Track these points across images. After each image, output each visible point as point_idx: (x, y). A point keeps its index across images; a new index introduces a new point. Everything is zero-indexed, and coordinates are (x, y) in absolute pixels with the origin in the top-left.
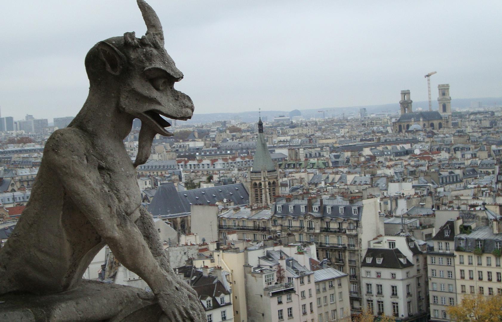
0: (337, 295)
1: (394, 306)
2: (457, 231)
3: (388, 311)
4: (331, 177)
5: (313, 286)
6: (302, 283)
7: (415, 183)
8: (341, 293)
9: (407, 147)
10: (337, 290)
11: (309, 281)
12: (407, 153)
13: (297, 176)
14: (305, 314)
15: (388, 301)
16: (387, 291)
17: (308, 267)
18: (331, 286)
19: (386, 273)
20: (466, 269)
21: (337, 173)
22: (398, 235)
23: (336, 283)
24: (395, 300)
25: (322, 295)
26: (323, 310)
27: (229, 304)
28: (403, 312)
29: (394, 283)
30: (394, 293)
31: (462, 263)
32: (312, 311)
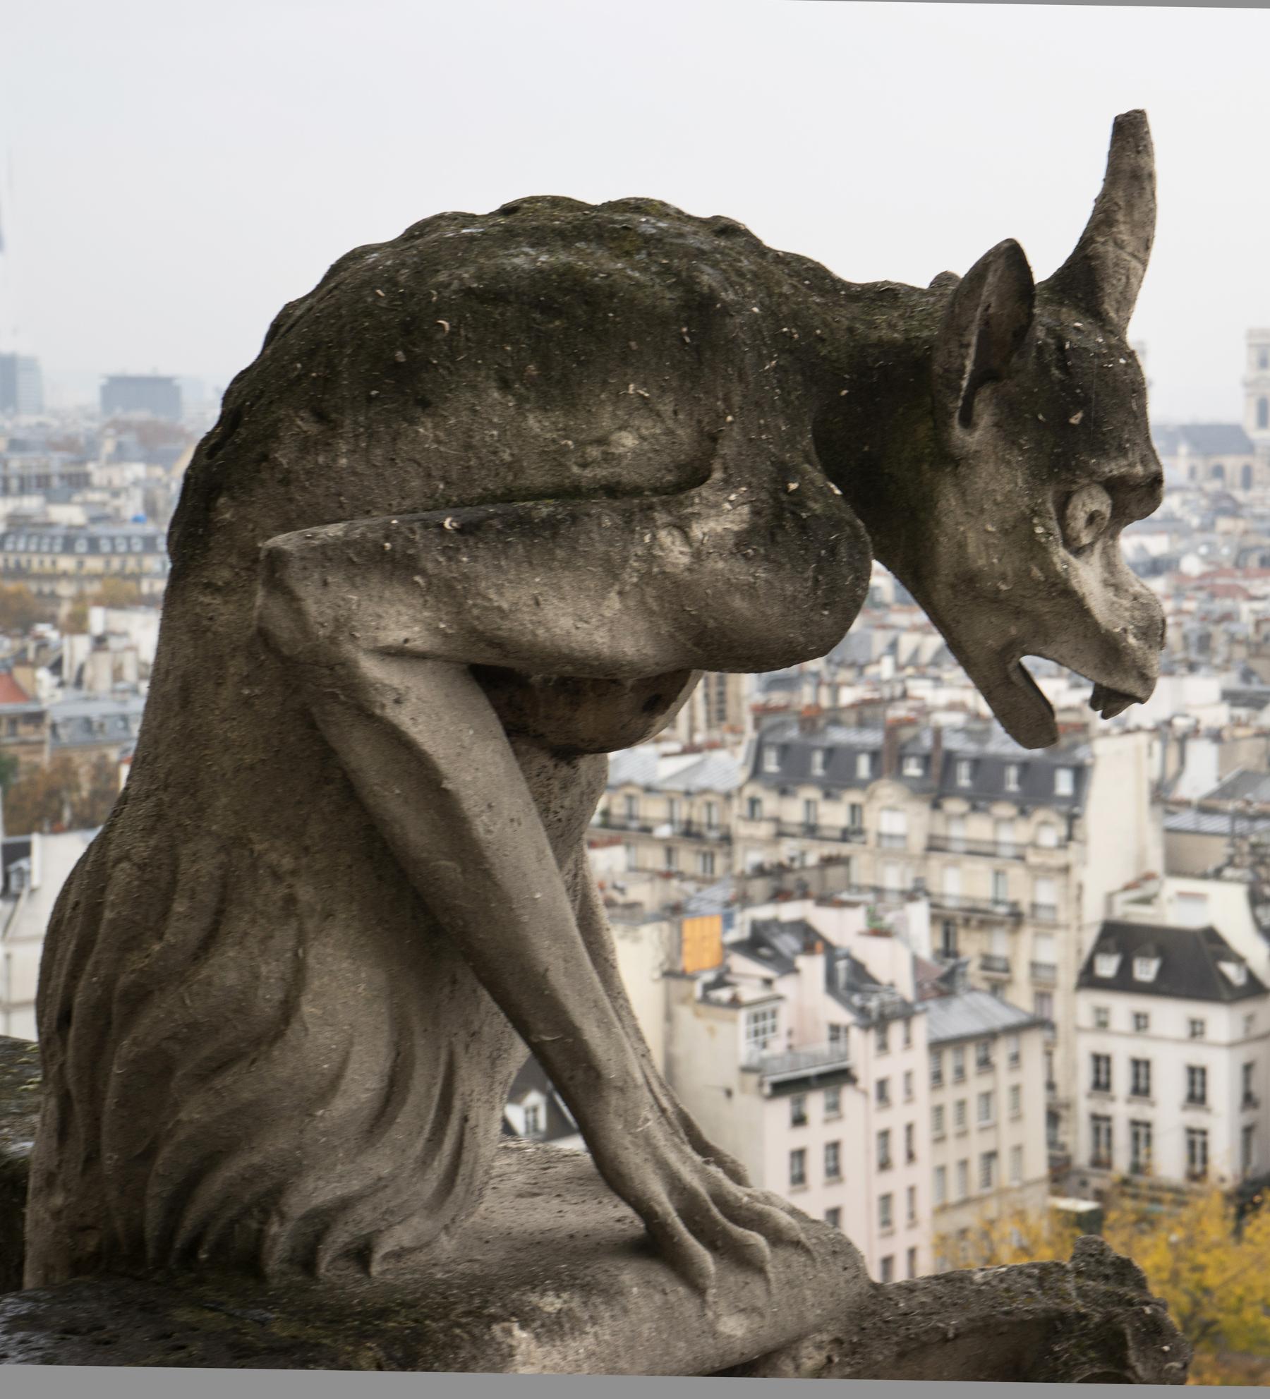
0: (1003, 1100)
1: (1192, 1145)
5: (919, 1060)
8: (1016, 1090)
10: (1004, 1077)
11: (908, 1041)
14: (885, 1165)
15: (1168, 1114)
16: (1169, 1085)
17: (906, 989)
18: (985, 1064)
19: (1170, 1015)
22: (1217, 875)
23: (1001, 1053)
24: (1196, 1118)
25: (949, 1096)
26: (952, 1153)
28: (1224, 1161)
29: (1197, 1054)
32: (911, 1156)
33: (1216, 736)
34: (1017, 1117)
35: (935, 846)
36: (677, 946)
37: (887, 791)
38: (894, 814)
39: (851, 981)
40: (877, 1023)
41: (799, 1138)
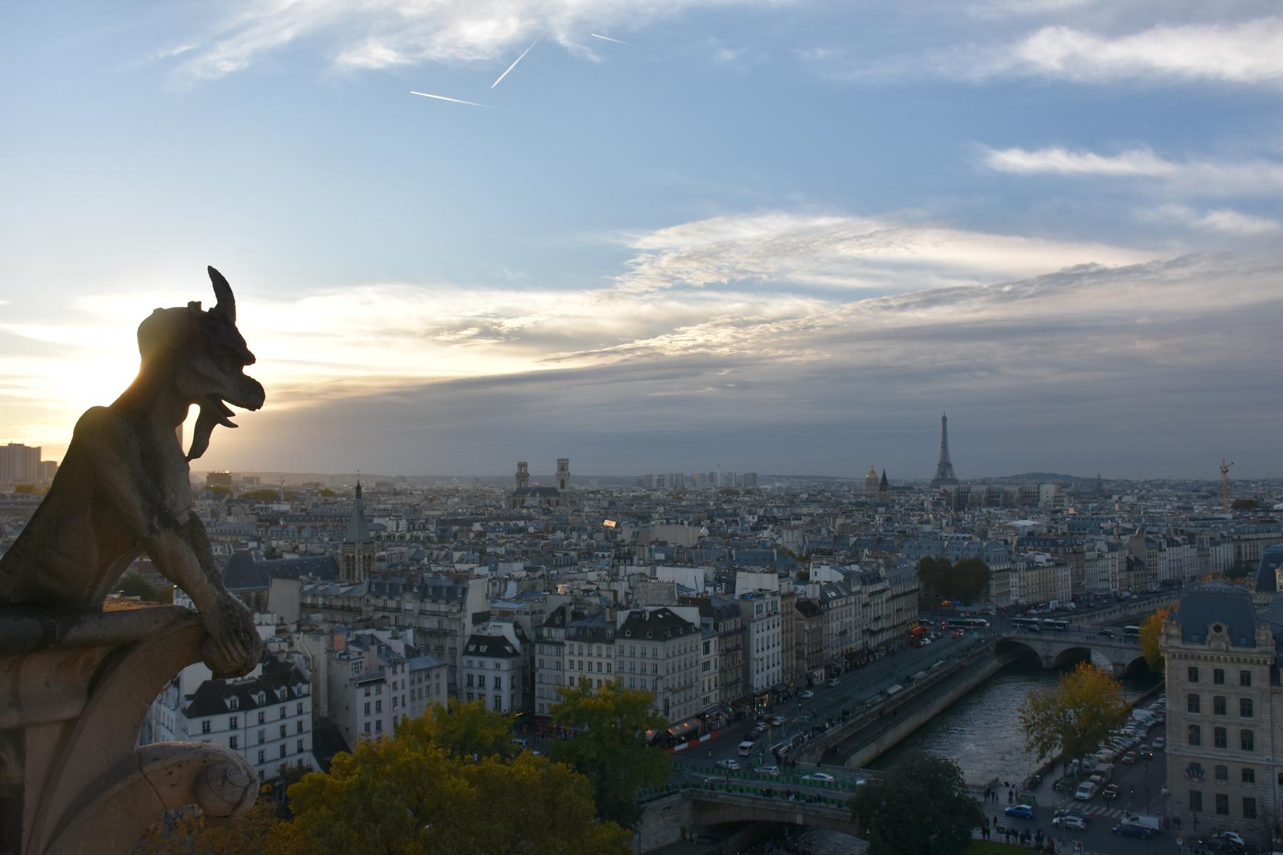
2: (569, 618)
3: (490, 704)
4: (435, 553)
5: (406, 676)
6: (395, 672)
7: (528, 563)
9: (521, 524)
10: (434, 681)
11: (403, 671)
12: (521, 530)
13: (397, 550)
16: (490, 683)
17: (403, 654)
18: (428, 677)
19: (490, 662)
20: (576, 659)
21: (442, 549)
23: (433, 673)
25: (416, 687)
27: (307, 695)
28: (505, 705)
29: (498, 674)
30: (498, 686)
31: (571, 653)
32: (404, 705)
33: (519, 580)
34: (438, 693)
35: (422, 612)
36: (332, 642)
37: (408, 596)
38: (410, 604)
39: (385, 651)
40: (394, 664)
41: (368, 699)
